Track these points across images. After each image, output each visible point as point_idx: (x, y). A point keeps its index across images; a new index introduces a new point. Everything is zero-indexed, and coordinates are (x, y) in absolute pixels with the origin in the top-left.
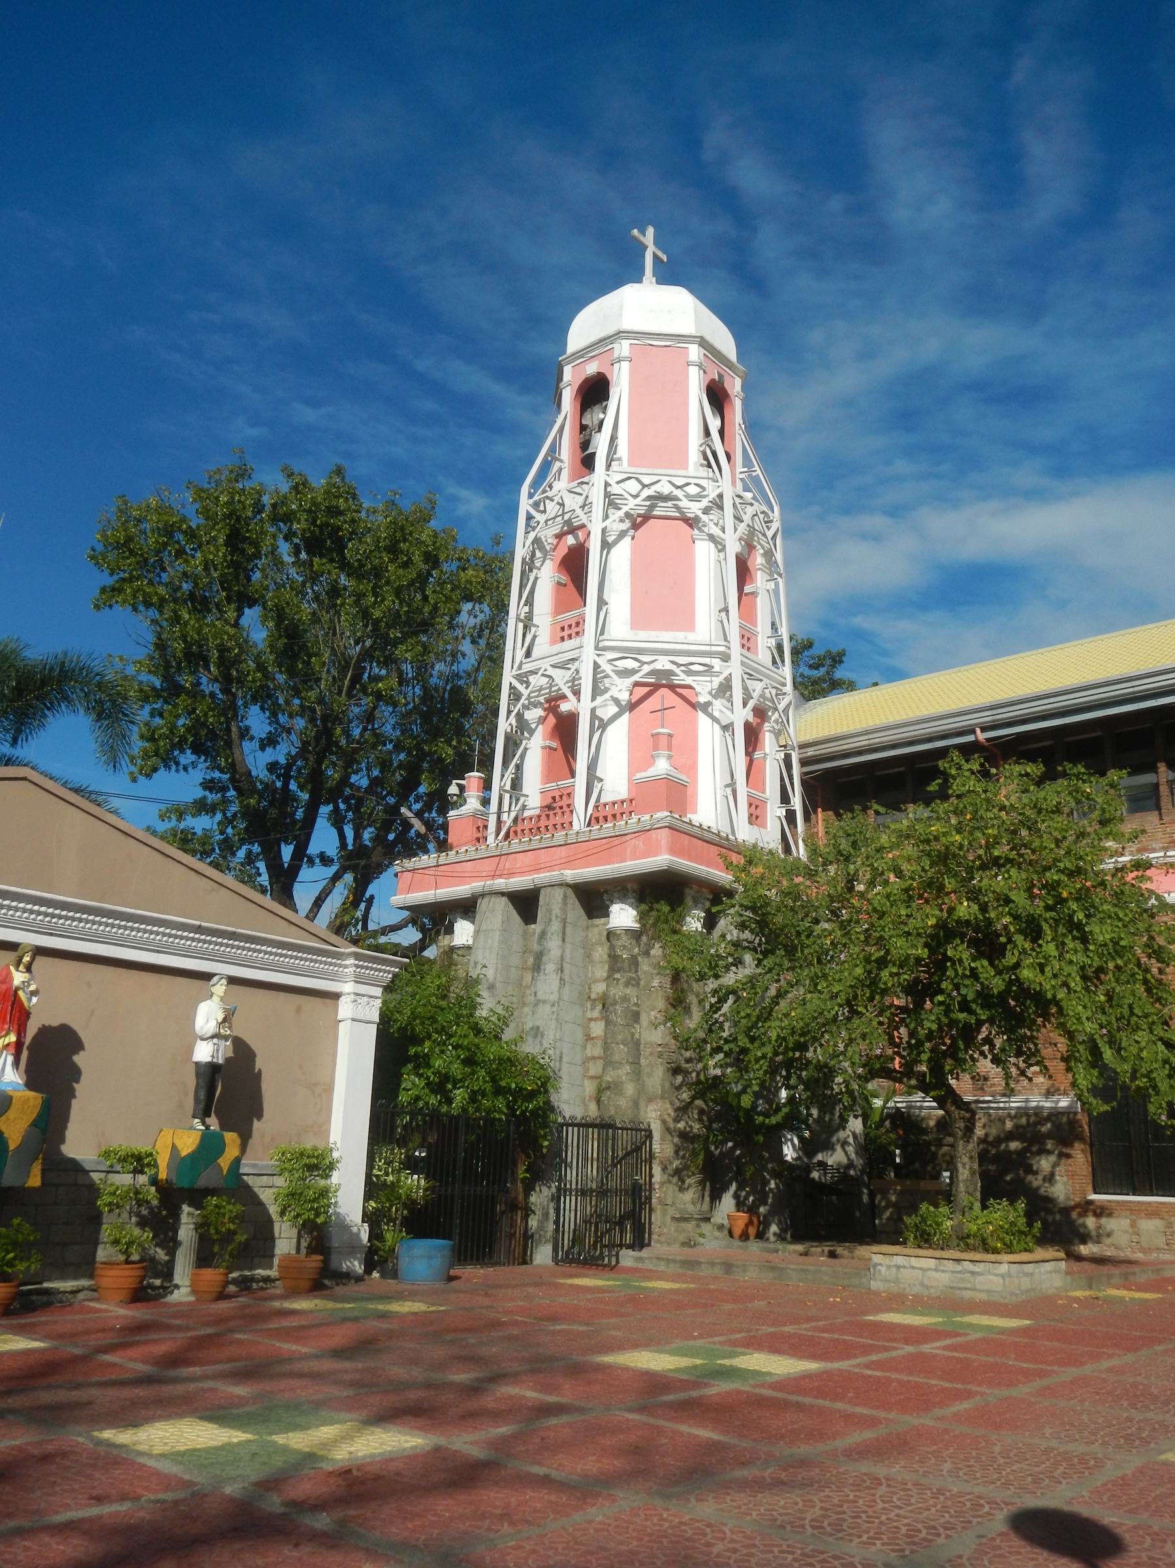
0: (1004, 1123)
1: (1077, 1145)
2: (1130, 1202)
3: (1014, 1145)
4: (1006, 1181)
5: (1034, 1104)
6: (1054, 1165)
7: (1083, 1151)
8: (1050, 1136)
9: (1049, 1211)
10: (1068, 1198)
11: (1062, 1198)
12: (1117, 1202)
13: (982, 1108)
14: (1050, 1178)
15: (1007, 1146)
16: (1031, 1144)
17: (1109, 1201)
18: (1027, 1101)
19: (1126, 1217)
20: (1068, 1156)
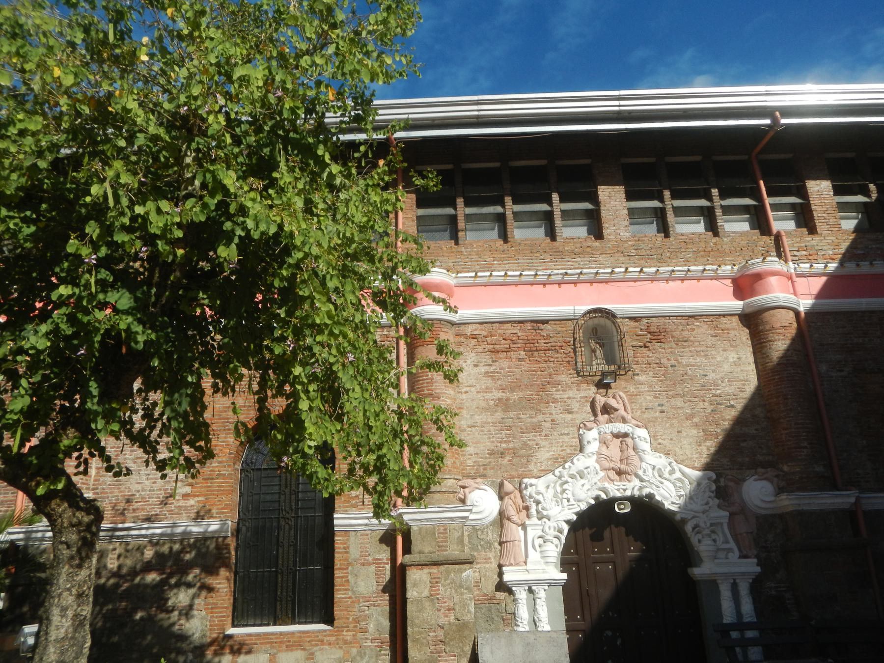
0: (143, 554)
1: (223, 572)
2: (272, 634)
3: (152, 577)
4: (135, 621)
5: (179, 530)
6: (194, 597)
7: (228, 579)
8: (191, 565)
9: (180, 652)
10: (204, 636)
11: (197, 635)
12: (258, 635)
13: (119, 537)
14: (187, 612)
15: (143, 579)
16: (171, 575)
17: (250, 635)
18: (174, 525)
19: (266, 652)
20: (210, 589)
